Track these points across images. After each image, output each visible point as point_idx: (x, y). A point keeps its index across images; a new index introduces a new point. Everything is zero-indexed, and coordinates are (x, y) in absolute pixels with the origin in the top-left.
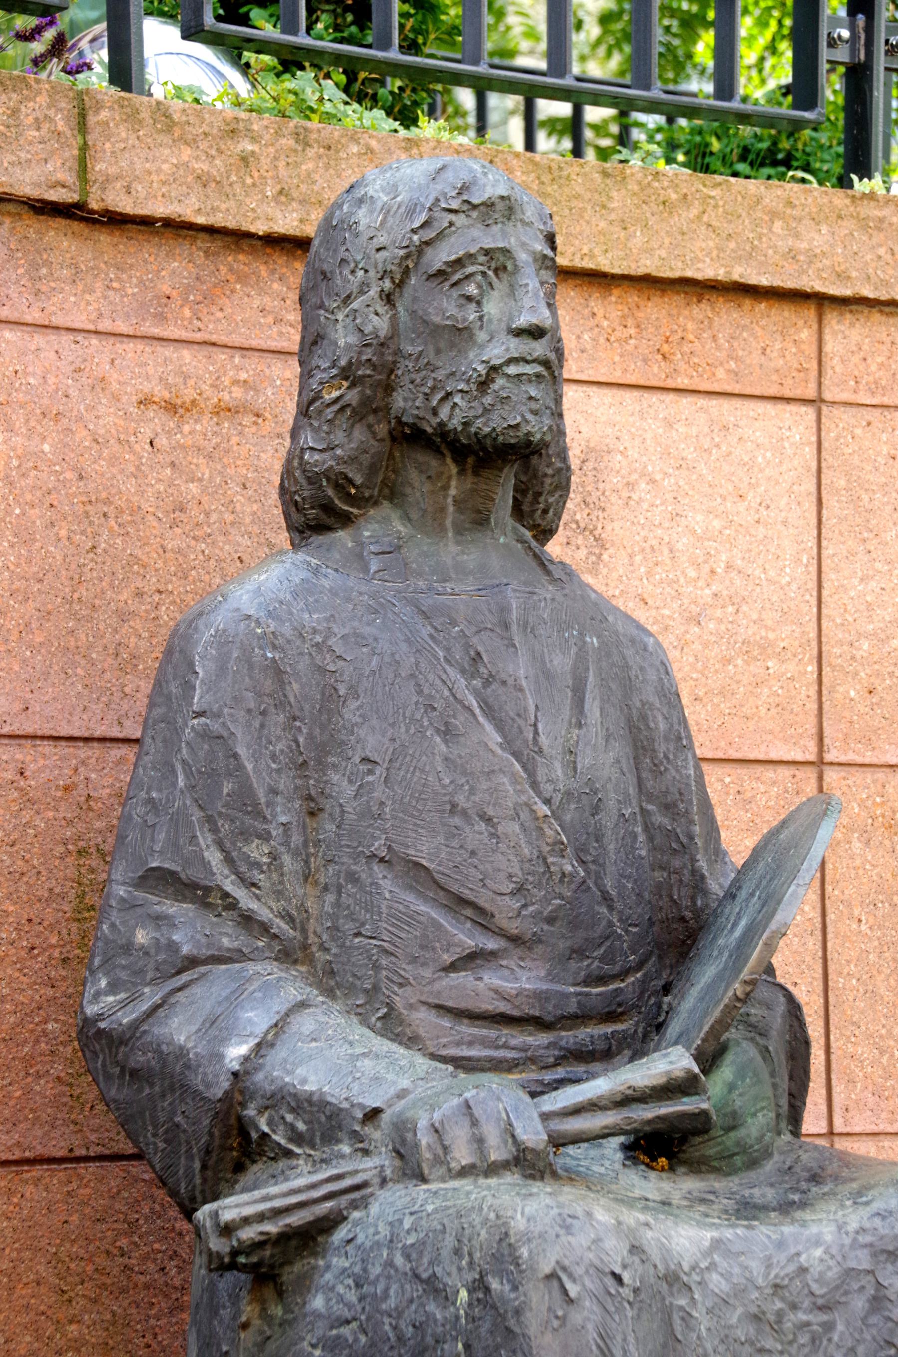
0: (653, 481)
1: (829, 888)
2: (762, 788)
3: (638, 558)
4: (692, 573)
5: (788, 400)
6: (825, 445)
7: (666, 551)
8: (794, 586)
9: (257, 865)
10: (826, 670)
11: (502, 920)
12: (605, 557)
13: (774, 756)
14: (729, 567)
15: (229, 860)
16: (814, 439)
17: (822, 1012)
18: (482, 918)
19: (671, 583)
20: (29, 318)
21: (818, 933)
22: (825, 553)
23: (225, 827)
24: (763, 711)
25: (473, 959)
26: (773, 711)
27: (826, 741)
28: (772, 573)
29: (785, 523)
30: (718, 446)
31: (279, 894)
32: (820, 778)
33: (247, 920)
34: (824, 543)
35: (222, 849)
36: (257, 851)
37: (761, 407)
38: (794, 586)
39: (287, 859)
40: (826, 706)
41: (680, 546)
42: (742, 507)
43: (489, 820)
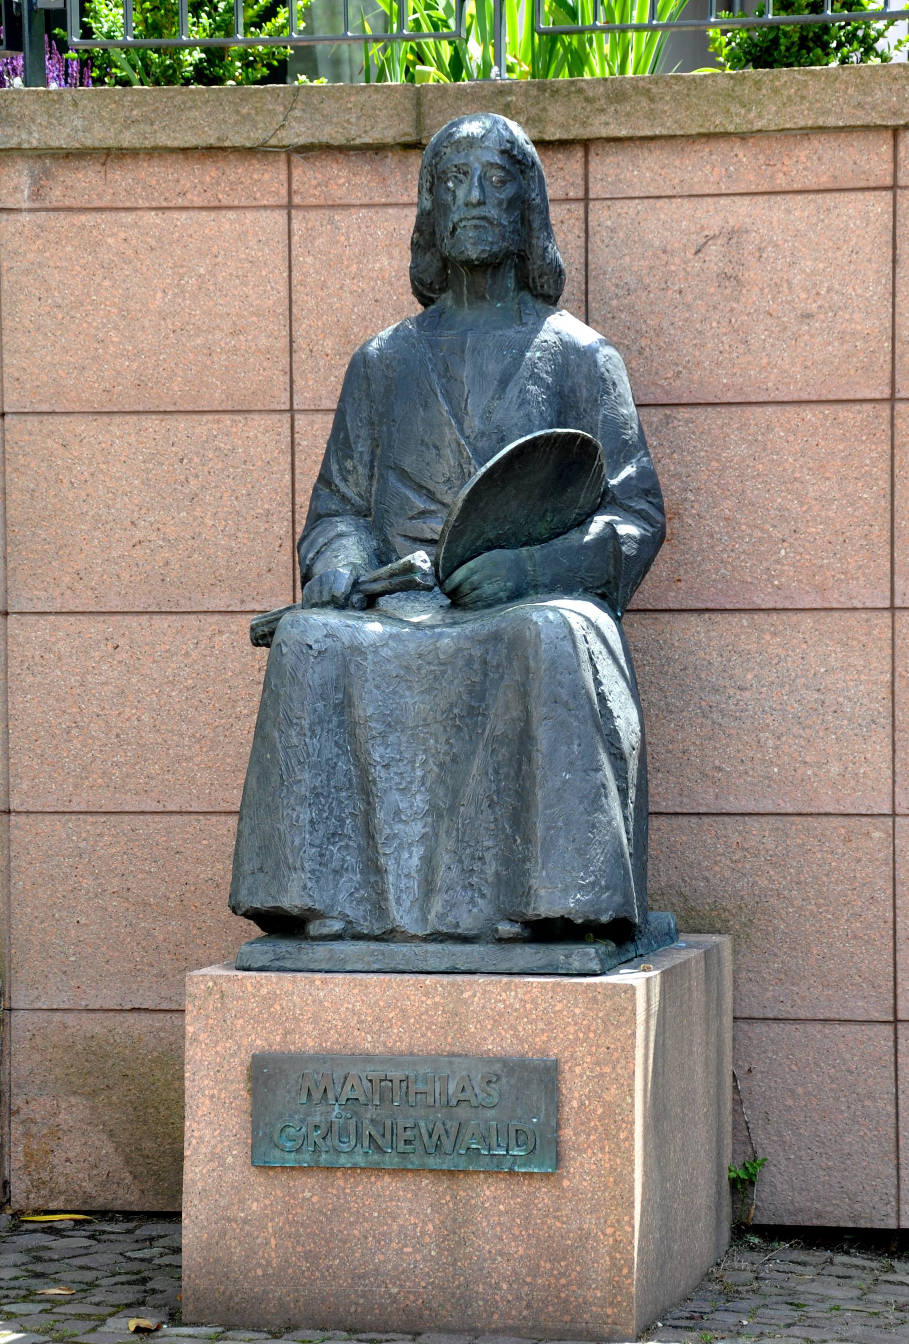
0: (777, 246)
1: (897, 471)
2: (851, 416)
3: (766, 290)
4: (803, 296)
5: (875, 189)
6: (899, 212)
7: (785, 285)
8: (875, 298)
9: (349, 471)
10: (898, 345)
11: (439, 496)
12: (744, 291)
13: (859, 396)
14: (829, 290)
15: (340, 470)
16: (891, 209)
17: (889, 540)
18: (431, 495)
19: (788, 303)
20: (401, 201)
21: (889, 497)
22: (898, 277)
23: (340, 454)
24: (852, 372)
25: (423, 514)
26: (860, 371)
27: (897, 386)
28: (859, 291)
29: (869, 261)
30: (823, 221)
31: (357, 485)
32: (893, 409)
33: (344, 498)
34: (898, 270)
35: (339, 465)
36: (349, 464)
37: (853, 195)
38: (875, 298)
39: (360, 469)
40: (898, 366)
41: (795, 281)
42: (839, 254)
43: (436, 447)
